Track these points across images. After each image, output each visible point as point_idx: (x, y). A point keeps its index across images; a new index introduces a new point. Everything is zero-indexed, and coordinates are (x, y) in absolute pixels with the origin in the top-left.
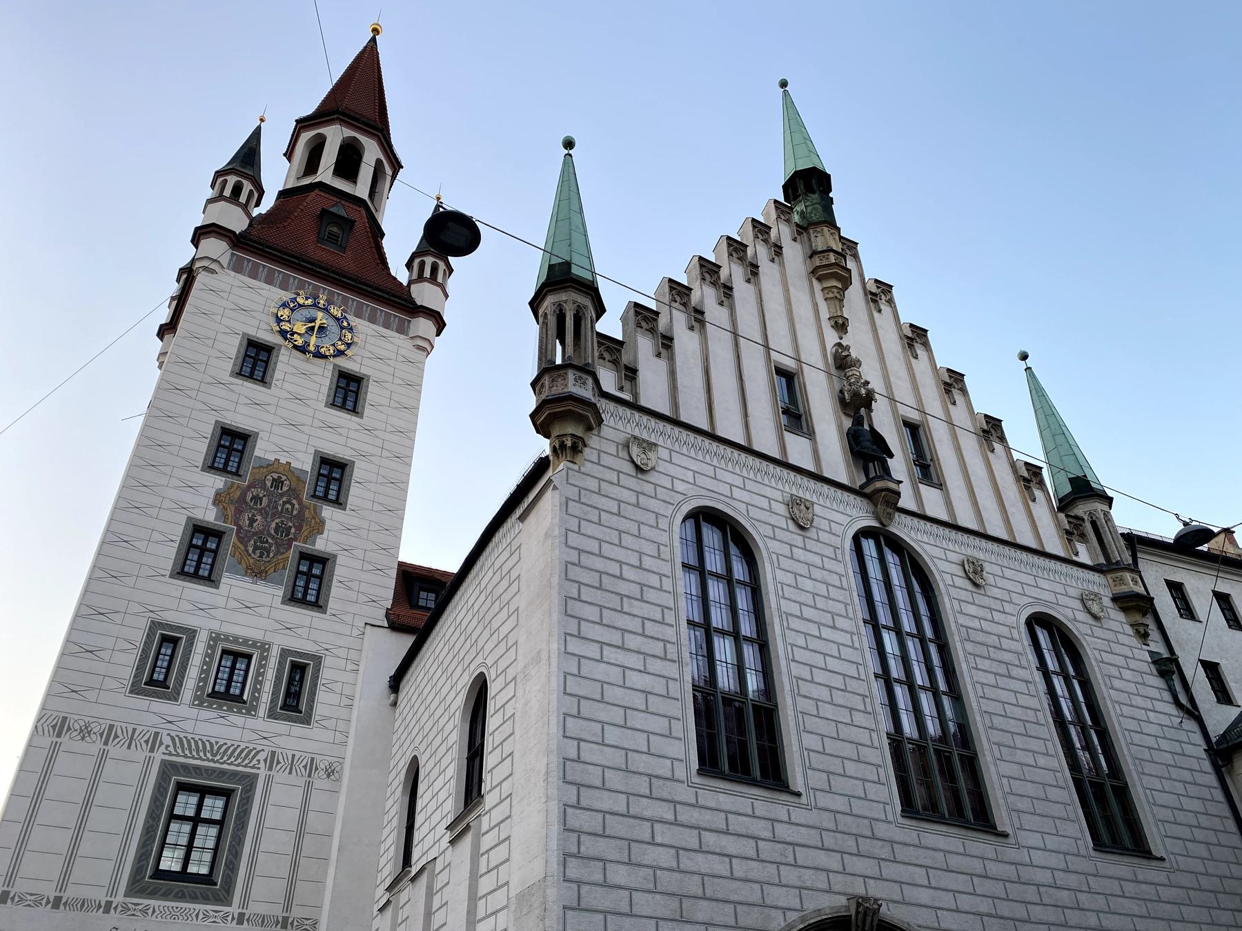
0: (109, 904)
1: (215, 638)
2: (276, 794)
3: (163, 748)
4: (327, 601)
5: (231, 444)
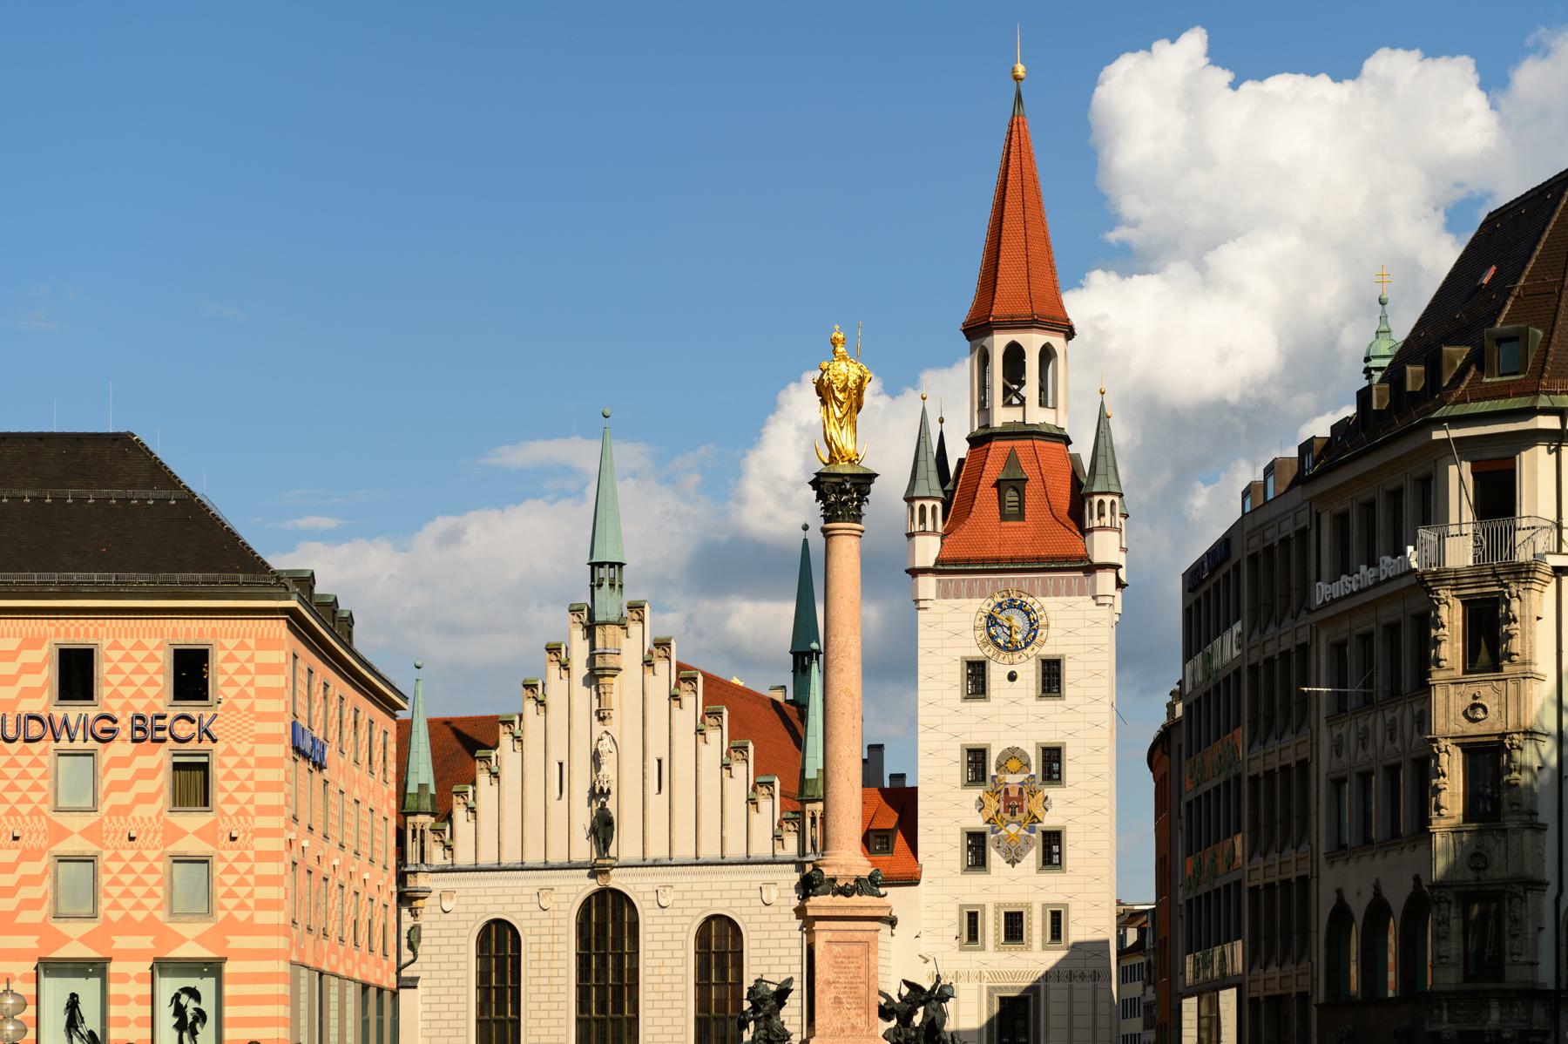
1: (998, 906)
2: (1052, 994)
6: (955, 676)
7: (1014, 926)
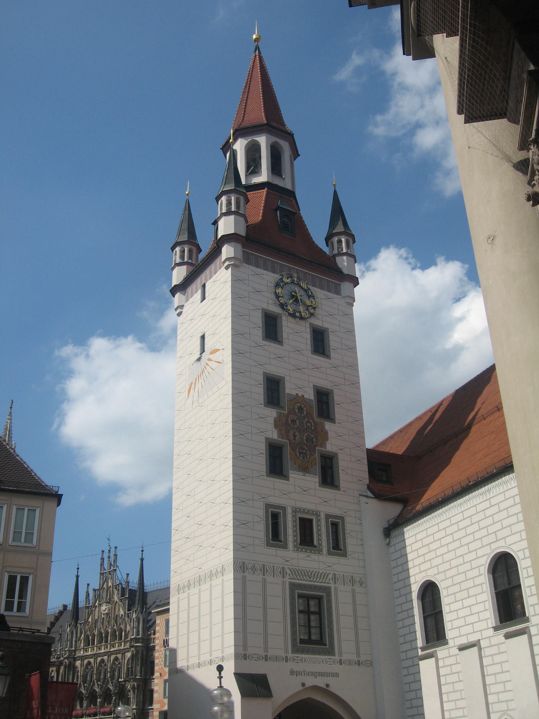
0: (286, 657)
1: (295, 511)
3: (288, 575)
4: (339, 483)
5: (273, 388)
6: (258, 319)
7: (306, 528)
